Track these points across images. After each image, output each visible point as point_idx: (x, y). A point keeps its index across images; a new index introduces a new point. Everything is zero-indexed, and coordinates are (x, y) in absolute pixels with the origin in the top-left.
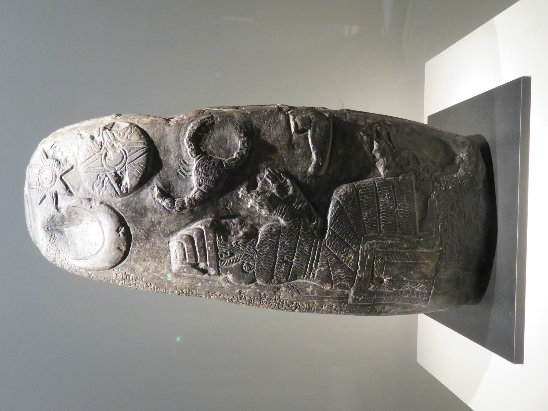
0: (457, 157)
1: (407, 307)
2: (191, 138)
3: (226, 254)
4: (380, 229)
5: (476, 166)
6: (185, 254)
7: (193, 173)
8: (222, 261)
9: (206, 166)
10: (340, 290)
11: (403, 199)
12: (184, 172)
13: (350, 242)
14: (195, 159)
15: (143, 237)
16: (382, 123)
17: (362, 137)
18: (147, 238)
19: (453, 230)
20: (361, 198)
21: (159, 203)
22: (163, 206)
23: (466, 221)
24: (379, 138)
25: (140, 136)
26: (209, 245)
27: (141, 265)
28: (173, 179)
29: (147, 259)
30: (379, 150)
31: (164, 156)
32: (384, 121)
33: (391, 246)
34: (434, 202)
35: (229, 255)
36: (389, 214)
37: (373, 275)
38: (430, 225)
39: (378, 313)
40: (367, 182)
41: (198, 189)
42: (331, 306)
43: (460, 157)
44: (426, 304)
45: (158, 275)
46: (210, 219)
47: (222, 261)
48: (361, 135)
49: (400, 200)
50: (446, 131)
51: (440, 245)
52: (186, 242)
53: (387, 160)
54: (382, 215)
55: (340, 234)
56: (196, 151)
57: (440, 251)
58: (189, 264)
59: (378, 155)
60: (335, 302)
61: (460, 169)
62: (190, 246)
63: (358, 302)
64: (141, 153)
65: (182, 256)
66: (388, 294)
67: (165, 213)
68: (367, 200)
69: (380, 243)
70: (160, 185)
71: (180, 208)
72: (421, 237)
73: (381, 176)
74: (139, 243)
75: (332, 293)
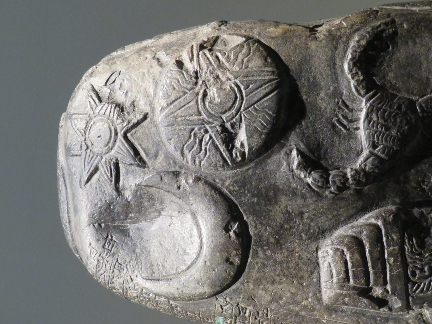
2: (357, 61)
3: (422, 270)
6: (347, 272)
7: (361, 124)
8: (414, 283)
9: (385, 111)
12: (345, 122)
14: (364, 100)
15: (272, 240)
18: (278, 242)
21: (300, 179)
22: (308, 184)
25: (266, 60)
26: (390, 255)
27: (266, 290)
28: (325, 135)
29: (278, 279)
31: (308, 94)
35: (427, 273)
41: (371, 154)
45: (297, 309)
46: (393, 208)
47: (414, 283)
52: (349, 249)
56: (366, 84)
58: (354, 288)
62: (357, 256)
64: (268, 90)
65: (342, 275)
67: (311, 197)
70: (302, 146)
71: (338, 188)
74: (264, 251)
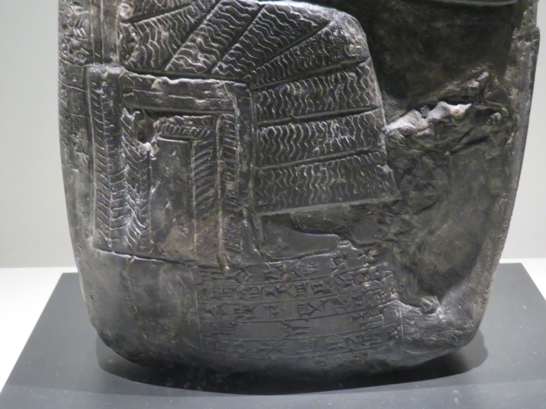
0: (435, 301)
1: (87, 204)
4: (267, 126)
5: (417, 344)
10: (118, 43)
11: (336, 176)
13: (232, 55)
16: (509, 124)
17: (475, 76)
19: (271, 294)
20: (336, 80)
23: (293, 324)
24: (478, 116)
30: (449, 117)
32: (514, 128)
33: (228, 153)
34: (333, 248)
36: (302, 144)
37: (158, 115)
38: (280, 240)
39: (69, 139)
40: (374, 90)
42: (78, 26)
43: (437, 306)
44: (96, 246)
48: (481, 73)
49: (334, 170)
50: (495, 275)
51: (234, 267)
53: (425, 136)
54: (298, 129)
55: (251, 31)
57: (222, 267)
59: (436, 114)
60: (89, 34)
61: (410, 308)
63: (92, 87)
66: (114, 156)
68: (332, 91)
69: (232, 126)
72: (250, 220)
73: (388, 123)
75: (111, 24)
